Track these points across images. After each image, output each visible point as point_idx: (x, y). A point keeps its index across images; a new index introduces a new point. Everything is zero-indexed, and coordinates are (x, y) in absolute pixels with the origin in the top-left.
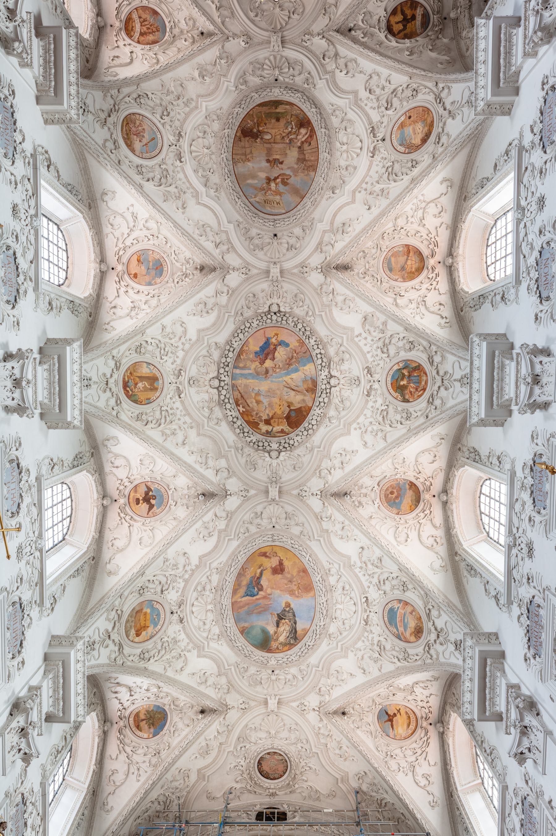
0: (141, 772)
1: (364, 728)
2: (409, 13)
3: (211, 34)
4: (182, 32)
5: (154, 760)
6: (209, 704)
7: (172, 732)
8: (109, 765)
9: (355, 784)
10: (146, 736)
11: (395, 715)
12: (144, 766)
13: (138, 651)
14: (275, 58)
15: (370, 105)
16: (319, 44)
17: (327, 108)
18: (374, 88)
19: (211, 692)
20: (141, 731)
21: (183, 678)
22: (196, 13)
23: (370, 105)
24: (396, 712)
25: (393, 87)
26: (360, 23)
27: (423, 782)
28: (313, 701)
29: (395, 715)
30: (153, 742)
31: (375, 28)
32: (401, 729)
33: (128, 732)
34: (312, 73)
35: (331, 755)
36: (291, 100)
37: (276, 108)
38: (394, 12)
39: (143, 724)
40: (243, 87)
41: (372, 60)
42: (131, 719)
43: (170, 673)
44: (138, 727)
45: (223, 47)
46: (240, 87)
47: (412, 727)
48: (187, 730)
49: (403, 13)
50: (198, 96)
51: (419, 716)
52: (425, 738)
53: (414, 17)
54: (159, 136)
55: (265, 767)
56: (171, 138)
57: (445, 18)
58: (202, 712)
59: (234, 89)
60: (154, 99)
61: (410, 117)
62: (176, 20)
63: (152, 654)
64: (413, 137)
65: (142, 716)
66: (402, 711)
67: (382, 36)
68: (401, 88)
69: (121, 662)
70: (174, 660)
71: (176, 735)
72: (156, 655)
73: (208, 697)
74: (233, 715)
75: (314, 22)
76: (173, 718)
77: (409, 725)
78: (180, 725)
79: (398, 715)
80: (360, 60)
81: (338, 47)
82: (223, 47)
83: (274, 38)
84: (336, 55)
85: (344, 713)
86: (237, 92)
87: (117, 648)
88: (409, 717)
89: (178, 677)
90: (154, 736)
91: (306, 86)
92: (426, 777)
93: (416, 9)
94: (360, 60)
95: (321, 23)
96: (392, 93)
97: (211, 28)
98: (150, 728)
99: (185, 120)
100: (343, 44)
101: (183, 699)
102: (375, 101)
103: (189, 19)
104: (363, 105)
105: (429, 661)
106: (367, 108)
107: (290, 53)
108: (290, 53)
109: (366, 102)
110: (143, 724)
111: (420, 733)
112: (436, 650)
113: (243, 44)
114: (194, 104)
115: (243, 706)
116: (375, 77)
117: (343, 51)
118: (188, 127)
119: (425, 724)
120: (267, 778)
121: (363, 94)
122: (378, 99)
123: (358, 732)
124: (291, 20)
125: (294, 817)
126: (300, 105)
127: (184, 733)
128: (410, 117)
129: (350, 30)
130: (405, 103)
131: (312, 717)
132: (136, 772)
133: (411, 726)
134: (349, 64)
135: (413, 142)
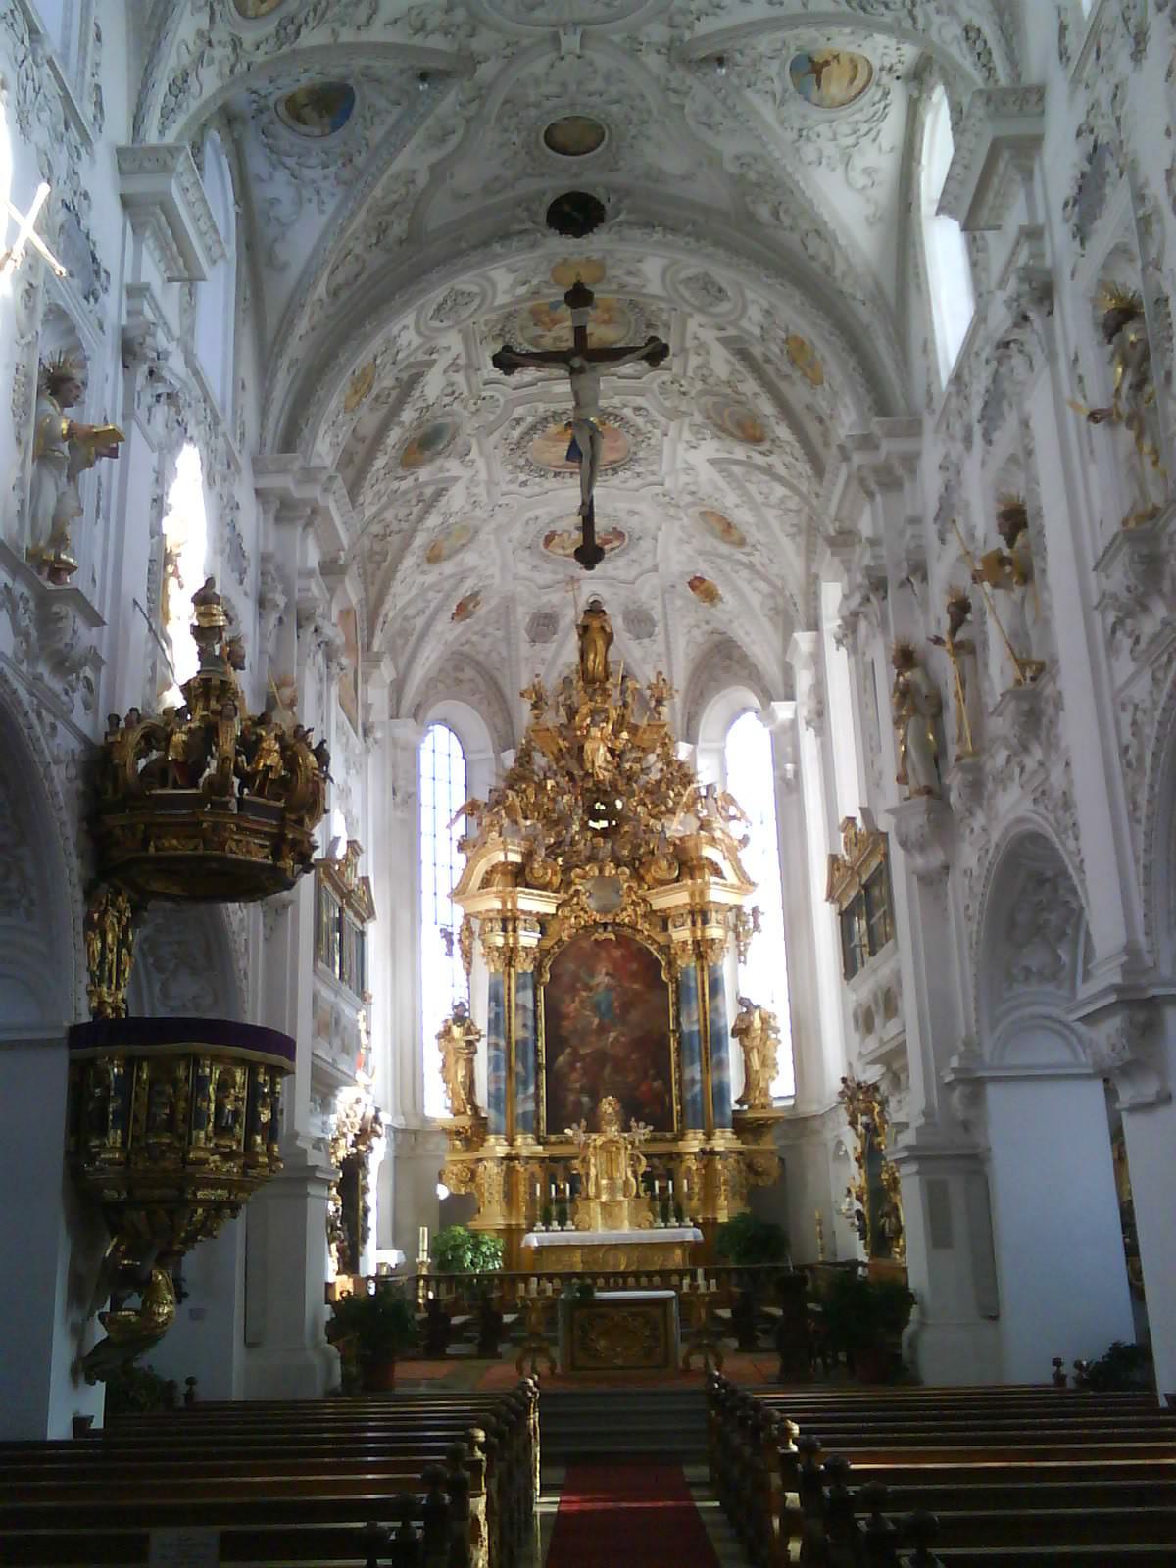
0: (324, 196)
1: (759, 85)
5: (346, 174)
6: (433, 64)
7: (368, 118)
8: (261, 193)
9: (732, 168)
10: (317, 131)
11: (827, 63)
12: (326, 186)
13: (271, 27)
19: (437, 42)
20: (305, 124)
21: (377, 34)
24: (830, 58)
27: (862, 181)
28: (658, 32)
29: (827, 63)
30: (334, 141)
32: (835, 86)
33: (279, 129)
35: (691, 122)
39: (307, 112)
42: (282, 109)
43: (347, 36)
44: (299, 118)
47: (859, 83)
48: (396, 111)
51: (876, 64)
52: (883, 104)
55: (560, 137)
58: (424, 77)
63: (302, 17)
65: (302, 100)
66: (844, 59)
69: (245, 65)
70: (350, 10)
71: (377, 120)
72: (310, 19)
73: (435, 52)
74: (486, 71)
76: (366, 96)
77: (852, 81)
78: (382, 103)
79: (834, 64)
85: (721, 61)
87: (229, 50)
88: (856, 67)
89: (365, 37)
90: (335, 127)
92: (868, 171)
98: (322, 116)
101: (381, 66)
105: (907, 24)
110: (307, 112)
111: (874, 93)
112: (927, 16)
115: (508, 52)
119: (886, 79)
120: (565, 152)
123: (749, 93)
125: (618, 213)
127: (391, 119)
131: (654, 61)
132: (315, 198)
133: (856, 83)
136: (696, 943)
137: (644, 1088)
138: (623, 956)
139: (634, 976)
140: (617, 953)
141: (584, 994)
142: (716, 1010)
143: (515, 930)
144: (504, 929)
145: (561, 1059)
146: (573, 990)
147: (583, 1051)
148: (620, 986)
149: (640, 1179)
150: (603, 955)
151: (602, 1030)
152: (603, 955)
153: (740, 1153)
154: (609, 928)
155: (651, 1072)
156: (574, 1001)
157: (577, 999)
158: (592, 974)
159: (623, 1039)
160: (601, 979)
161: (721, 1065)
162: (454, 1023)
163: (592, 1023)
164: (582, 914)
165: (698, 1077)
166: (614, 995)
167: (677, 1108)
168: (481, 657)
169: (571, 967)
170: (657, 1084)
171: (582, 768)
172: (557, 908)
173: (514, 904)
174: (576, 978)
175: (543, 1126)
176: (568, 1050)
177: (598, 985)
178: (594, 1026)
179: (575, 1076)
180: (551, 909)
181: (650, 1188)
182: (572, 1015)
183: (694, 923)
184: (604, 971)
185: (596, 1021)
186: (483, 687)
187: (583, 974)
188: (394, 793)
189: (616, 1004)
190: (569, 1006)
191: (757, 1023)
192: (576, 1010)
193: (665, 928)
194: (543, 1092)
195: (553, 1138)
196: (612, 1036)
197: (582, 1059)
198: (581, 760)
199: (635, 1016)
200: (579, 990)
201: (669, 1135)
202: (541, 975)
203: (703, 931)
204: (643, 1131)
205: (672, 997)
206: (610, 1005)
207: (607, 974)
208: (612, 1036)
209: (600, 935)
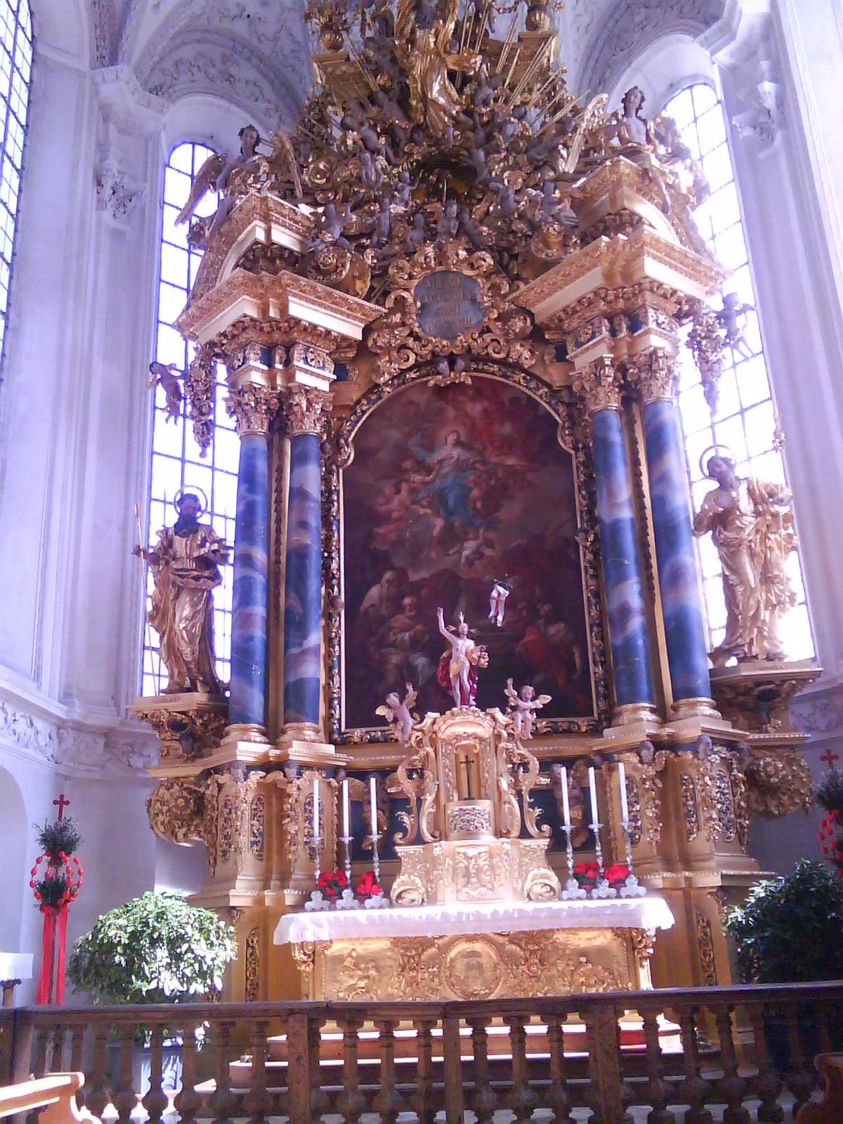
136: (621, 369)
137: (530, 637)
138: (485, 411)
139: (506, 445)
140: (476, 409)
141: (418, 478)
142: (660, 479)
143: (288, 362)
144: (269, 361)
145: (374, 592)
146: (396, 473)
147: (414, 577)
148: (483, 462)
149: (527, 799)
150: (451, 412)
151: (451, 538)
152: (451, 412)
153: (731, 745)
154: (461, 363)
155: (545, 608)
156: (398, 491)
157: (404, 487)
158: (430, 447)
159: (488, 552)
160: (449, 451)
161: (675, 578)
162: (176, 533)
163: (430, 528)
164: (410, 342)
165: (635, 601)
166: (470, 476)
167: (596, 671)
168: (266, 48)
169: (395, 435)
170: (556, 630)
171: (409, 119)
172: (367, 331)
173: (284, 309)
174: (404, 453)
175: (341, 711)
176: (388, 575)
177: (441, 462)
178: (436, 532)
179: (400, 620)
180: (354, 331)
181: (551, 816)
182: (395, 515)
183: (613, 332)
184: (452, 438)
185: (439, 523)
186: (269, 94)
187: (414, 445)
188: (99, 183)
189: (475, 493)
190: (388, 500)
191: (745, 505)
192: (402, 506)
193: (561, 355)
194: (341, 650)
195: (357, 733)
196: (469, 547)
197: (415, 588)
198: (403, 102)
199: (510, 511)
200: (407, 471)
201: (583, 723)
202: (338, 449)
203: (631, 345)
204: (530, 705)
205: (578, 478)
206: (464, 498)
207: (458, 443)
208: (469, 547)
209: (444, 376)
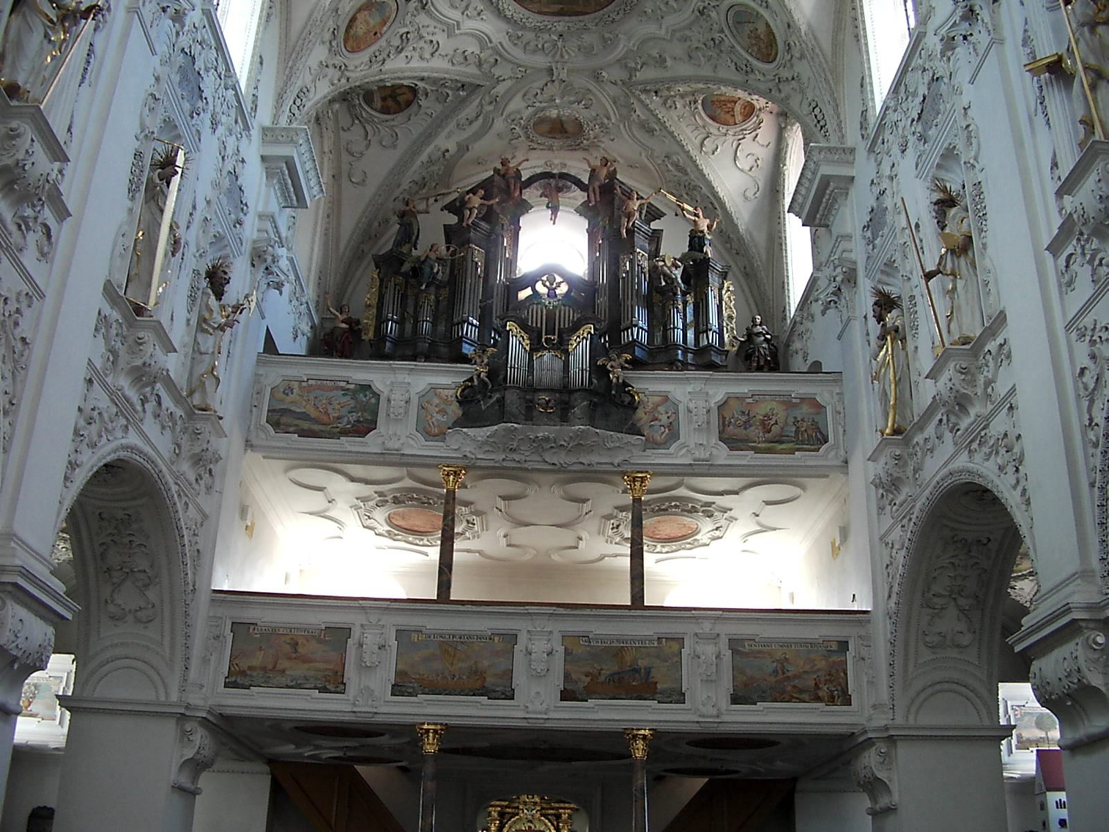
2: (390, 102)
3: (646, 91)
4: (683, 98)
14: (562, 56)
15: (431, 29)
16: (501, 71)
17: (489, 15)
18: (426, 46)
22: (662, 113)
23: (431, 29)
25: (403, 54)
26: (450, 93)
31: (432, 91)
34: (511, 45)
36: (540, 18)
37: (562, 8)
38: (409, 104)
40: (607, 35)
41: (433, 70)
45: (631, 76)
46: (611, 36)
49: (398, 103)
50: (670, 41)
53: (384, 99)
54: (730, 22)
56: (713, 14)
57: (344, 100)
59: (619, 35)
60: (729, 61)
61: (375, 34)
62: (687, 108)
64: (368, 17)
67: (420, 84)
68: (392, 57)
75: (510, 88)
80: (449, 66)
81: (479, 72)
82: (631, 76)
83: (564, 76)
84: (480, 65)
86: (617, 32)
91: (520, 33)
93: (382, 106)
94: (447, 66)
95: (501, 89)
96: (402, 49)
97: (643, 97)
99: (692, 23)
100: (473, 76)
102: (425, 35)
103: (671, 107)
104: (439, 26)
106: (433, 23)
107: (541, 61)
108: (541, 61)
109: (436, 30)
113: (604, 74)
114: (678, 35)
116: (427, 56)
117: (473, 70)
118: (686, 15)
121: (441, 38)
122: (421, 37)
124: (541, 86)
126: (527, 13)
128: (375, 34)
129: (463, 86)
130: (384, 44)
134: (463, 61)
135: (366, 12)
